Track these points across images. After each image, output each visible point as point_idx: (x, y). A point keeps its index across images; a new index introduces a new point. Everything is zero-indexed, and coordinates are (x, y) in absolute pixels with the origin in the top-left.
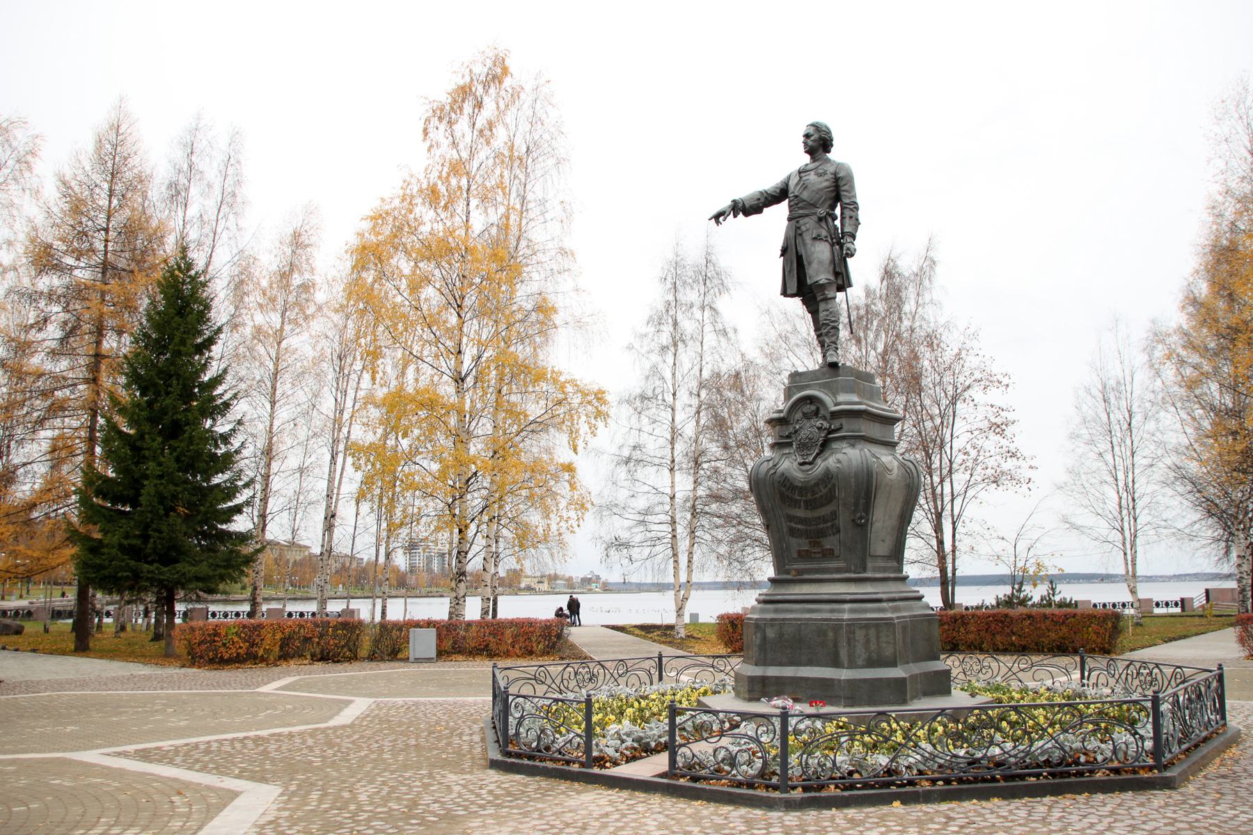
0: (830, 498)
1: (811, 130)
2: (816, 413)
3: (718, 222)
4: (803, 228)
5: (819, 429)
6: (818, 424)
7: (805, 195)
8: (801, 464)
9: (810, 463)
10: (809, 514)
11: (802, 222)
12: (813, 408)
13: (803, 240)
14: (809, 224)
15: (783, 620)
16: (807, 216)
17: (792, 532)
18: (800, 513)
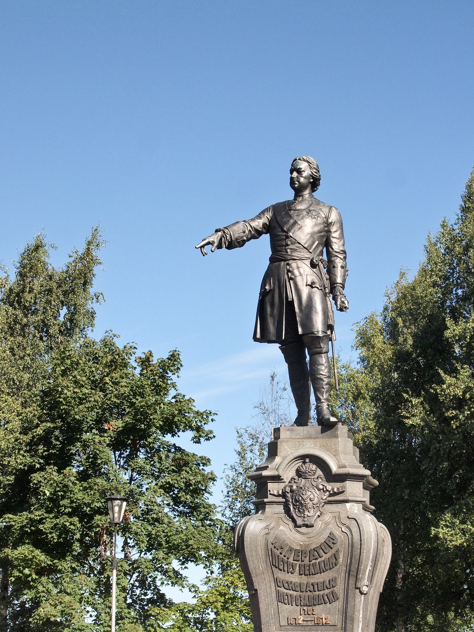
10: (304, 579)
18: (295, 578)
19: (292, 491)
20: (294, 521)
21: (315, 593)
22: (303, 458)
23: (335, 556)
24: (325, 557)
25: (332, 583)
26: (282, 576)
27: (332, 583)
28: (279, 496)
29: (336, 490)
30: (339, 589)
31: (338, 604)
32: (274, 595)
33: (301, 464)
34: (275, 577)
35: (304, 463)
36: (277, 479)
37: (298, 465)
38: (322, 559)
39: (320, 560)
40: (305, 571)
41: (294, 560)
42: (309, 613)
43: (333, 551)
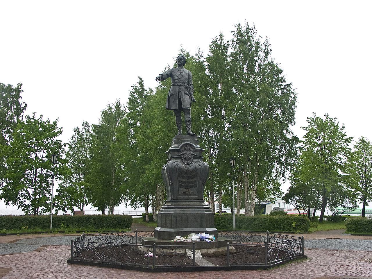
2: (189, 149)
3: (157, 81)
4: (182, 89)
6: (191, 153)
7: (183, 79)
8: (186, 165)
9: (190, 165)
10: (187, 181)
11: (181, 87)
12: (189, 148)
14: (183, 88)
15: (182, 213)
16: (183, 86)
17: (180, 186)
18: (184, 180)
19: (183, 154)
25: (195, 182)
28: (179, 156)
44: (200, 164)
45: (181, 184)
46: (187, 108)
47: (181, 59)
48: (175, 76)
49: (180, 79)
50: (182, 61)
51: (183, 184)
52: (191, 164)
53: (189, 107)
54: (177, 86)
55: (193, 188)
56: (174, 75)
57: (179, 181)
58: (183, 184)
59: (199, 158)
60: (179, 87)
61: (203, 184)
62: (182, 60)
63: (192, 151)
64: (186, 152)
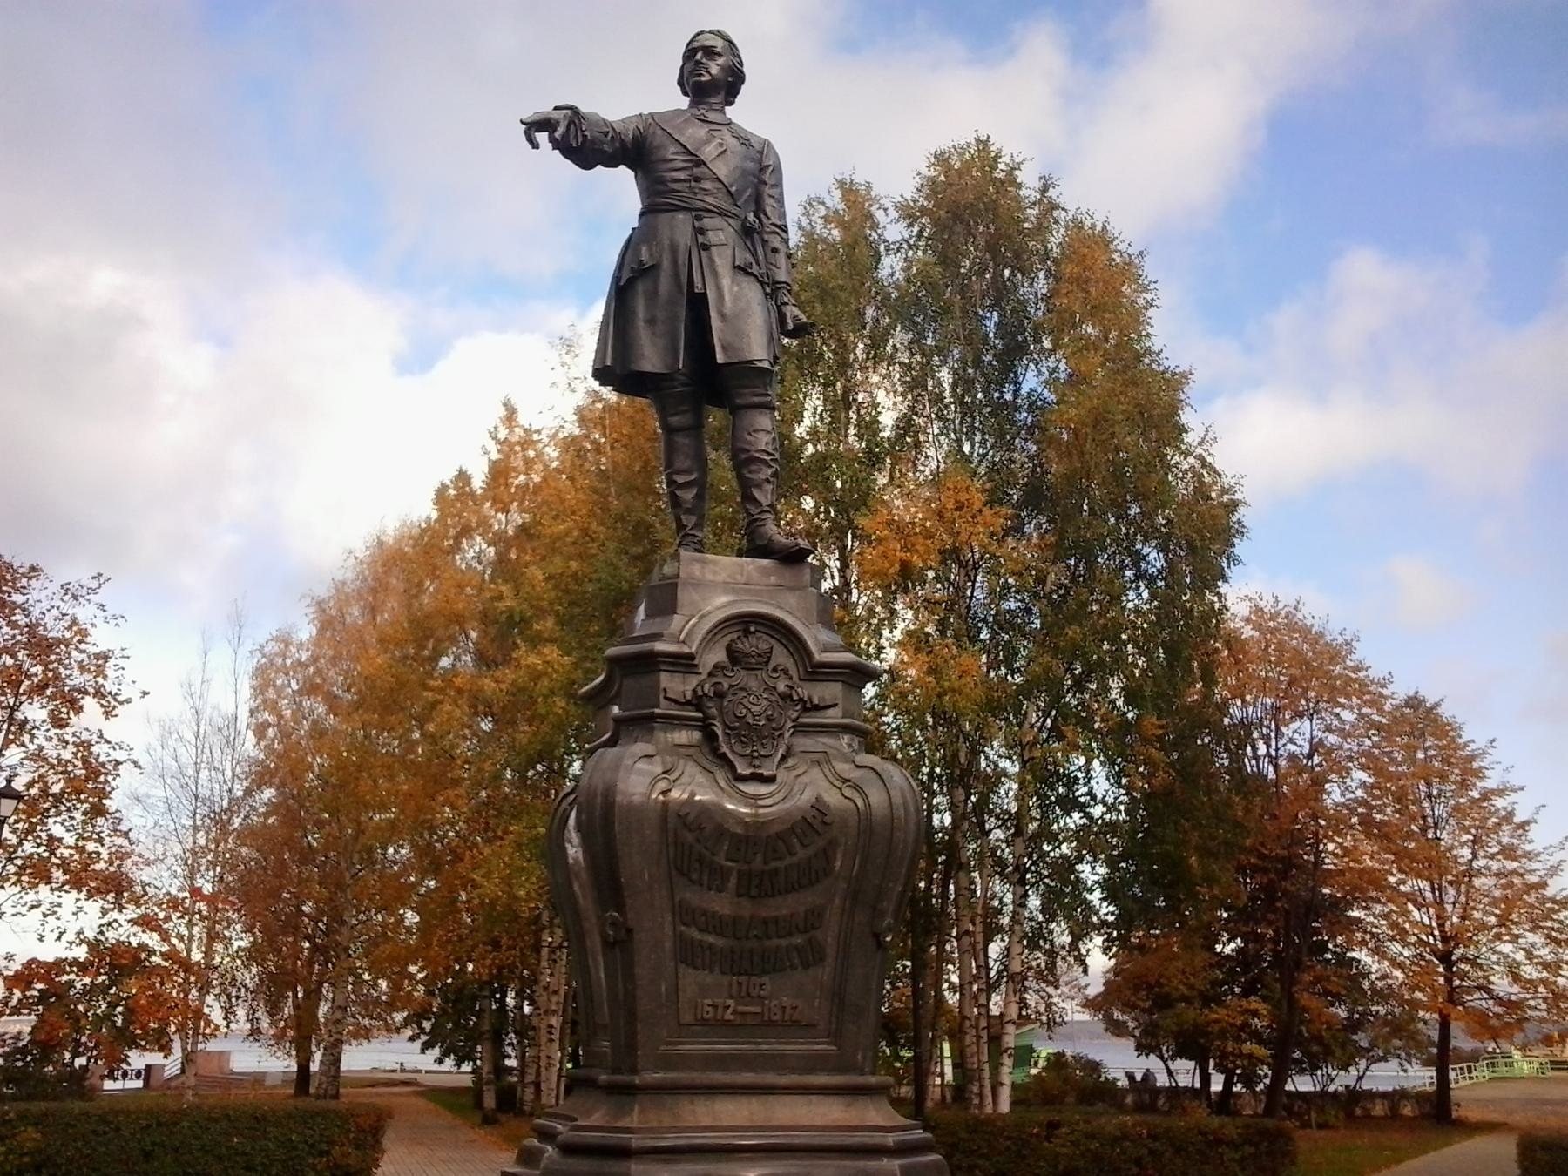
0: (814, 873)
1: (719, 44)
5: (785, 697)
6: (781, 687)
9: (771, 780)
10: (746, 908)
11: (708, 222)
13: (712, 260)
16: (722, 213)
17: (688, 954)
18: (721, 904)
19: (720, 695)
20: (732, 767)
21: (768, 943)
22: (745, 623)
23: (827, 854)
24: (801, 854)
25: (814, 919)
26: (691, 896)
27: (814, 919)
28: (688, 703)
29: (816, 701)
30: (829, 936)
31: (825, 973)
32: (668, 945)
33: (735, 636)
34: (677, 899)
35: (747, 633)
36: (684, 663)
37: (729, 638)
38: (795, 859)
39: (788, 861)
40: (757, 886)
41: (727, 859)
42: (754, 993)
43: (821, 843)
44: (844, 768)
45: (697, 935)
46: (751, 362)
47: (710, 52)
48: (671, 151)
49: (700, 163)
50: (720, 61)
51: (711, 939)
52: (782, 776)
53: (757, 350)
54: (681, 216)
55: (793, 968)
56: (659, 147)
57: (685, 914)
58: (711, 939)
59: (847, 729)
60: (699, 218)
61: (877, 936)
62: (720, 55)
63: (786, 672)
64: (741, 677)
